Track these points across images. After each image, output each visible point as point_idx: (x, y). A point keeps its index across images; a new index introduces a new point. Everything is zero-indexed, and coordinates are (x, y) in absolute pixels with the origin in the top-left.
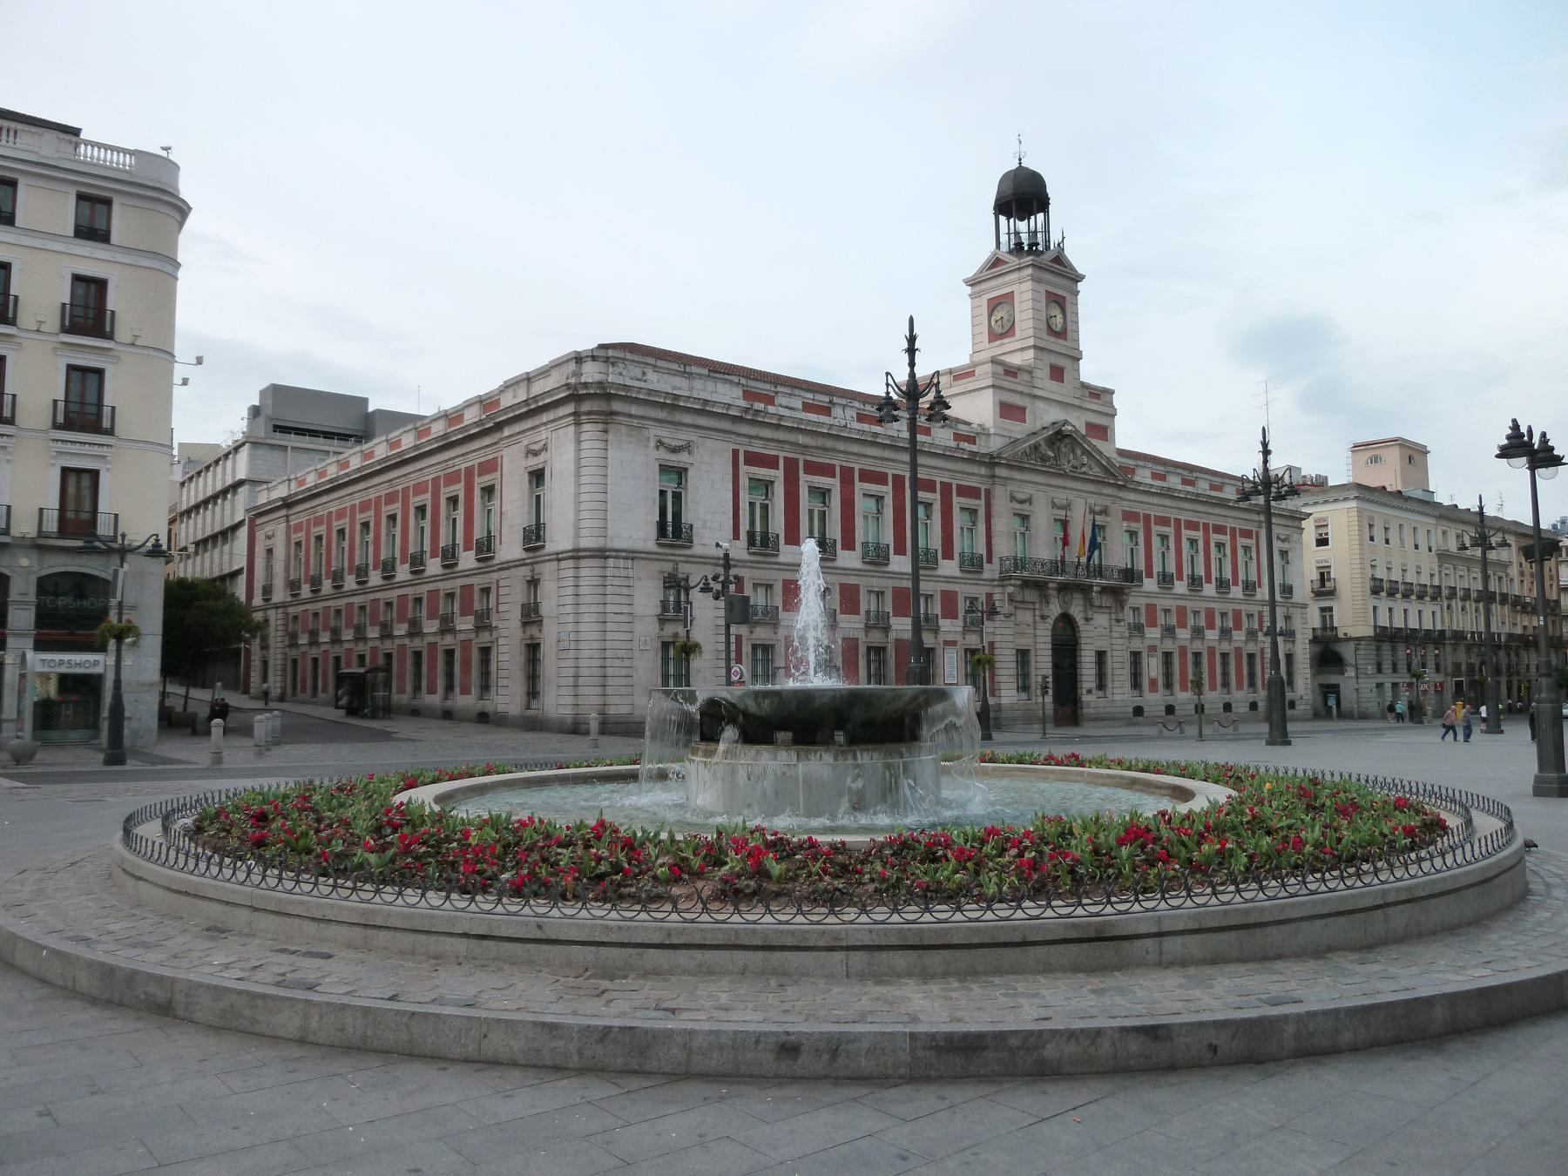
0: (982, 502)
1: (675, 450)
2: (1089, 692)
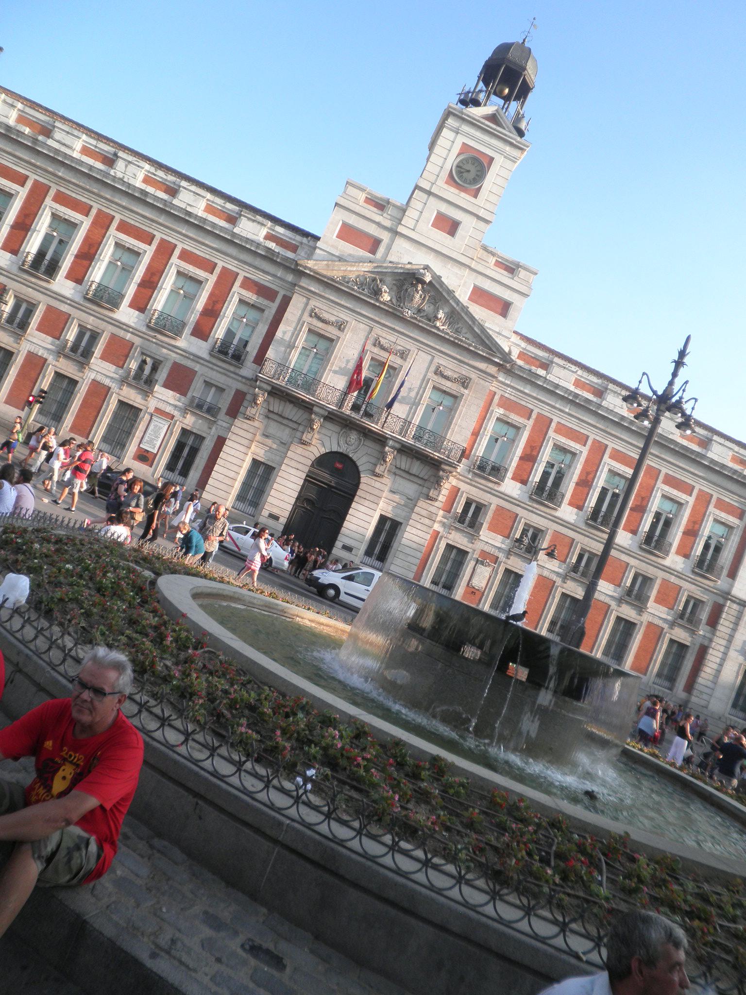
0: (274, 306)
2: (348, 548)
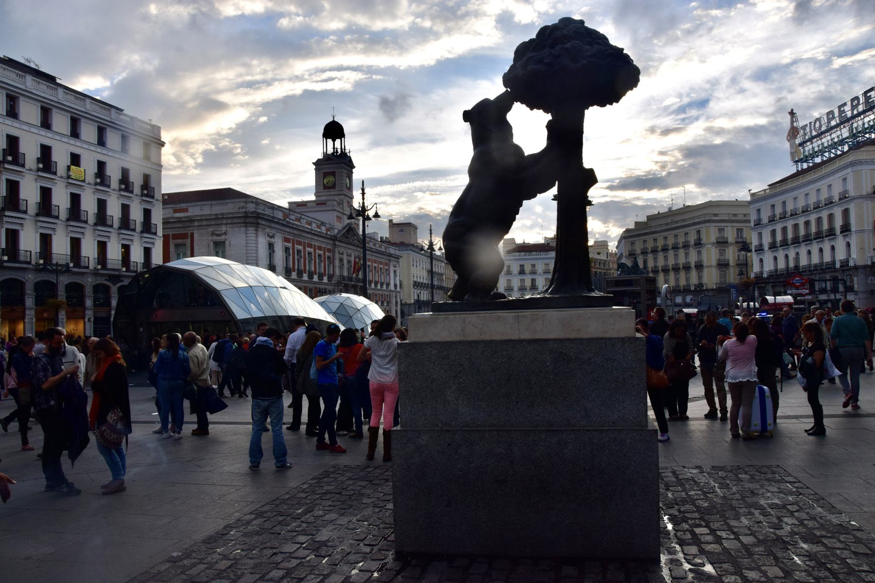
1: (271, 237)
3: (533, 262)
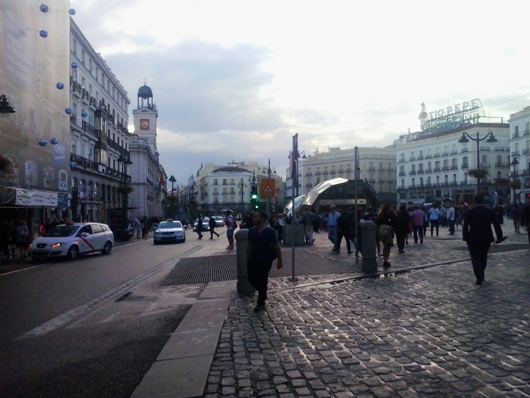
3: (232, 178)
